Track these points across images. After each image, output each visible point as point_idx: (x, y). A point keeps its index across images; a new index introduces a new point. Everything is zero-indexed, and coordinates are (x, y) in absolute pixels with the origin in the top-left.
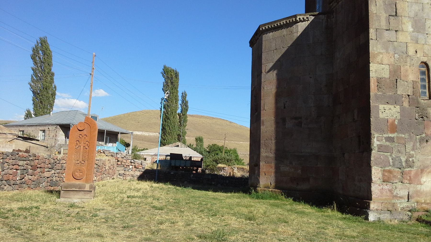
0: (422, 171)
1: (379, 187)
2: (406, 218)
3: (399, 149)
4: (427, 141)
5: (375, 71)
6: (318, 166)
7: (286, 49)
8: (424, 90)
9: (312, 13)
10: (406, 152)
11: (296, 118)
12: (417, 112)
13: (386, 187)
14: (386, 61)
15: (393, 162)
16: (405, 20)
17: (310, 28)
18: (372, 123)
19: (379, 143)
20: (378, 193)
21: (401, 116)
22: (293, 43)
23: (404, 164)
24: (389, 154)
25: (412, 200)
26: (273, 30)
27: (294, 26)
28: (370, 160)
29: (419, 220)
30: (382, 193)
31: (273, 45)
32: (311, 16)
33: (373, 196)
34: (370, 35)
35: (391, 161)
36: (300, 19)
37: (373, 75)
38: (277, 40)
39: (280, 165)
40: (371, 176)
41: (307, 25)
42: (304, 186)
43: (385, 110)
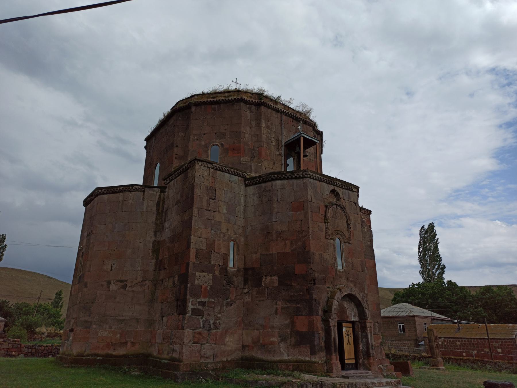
0: (226, 331)
1: (190, 349)
3: (209, 312)
5: (195, 243)
6: (138, 330)
10: (214, 315)
11: (121, 281)
12: (225, 280)
13: (196, 347)
14: (204, 236)
15: (203, 325)
20: (188, 355)
23: (212, 326)
35: (202, 323)
43: (201, 277)
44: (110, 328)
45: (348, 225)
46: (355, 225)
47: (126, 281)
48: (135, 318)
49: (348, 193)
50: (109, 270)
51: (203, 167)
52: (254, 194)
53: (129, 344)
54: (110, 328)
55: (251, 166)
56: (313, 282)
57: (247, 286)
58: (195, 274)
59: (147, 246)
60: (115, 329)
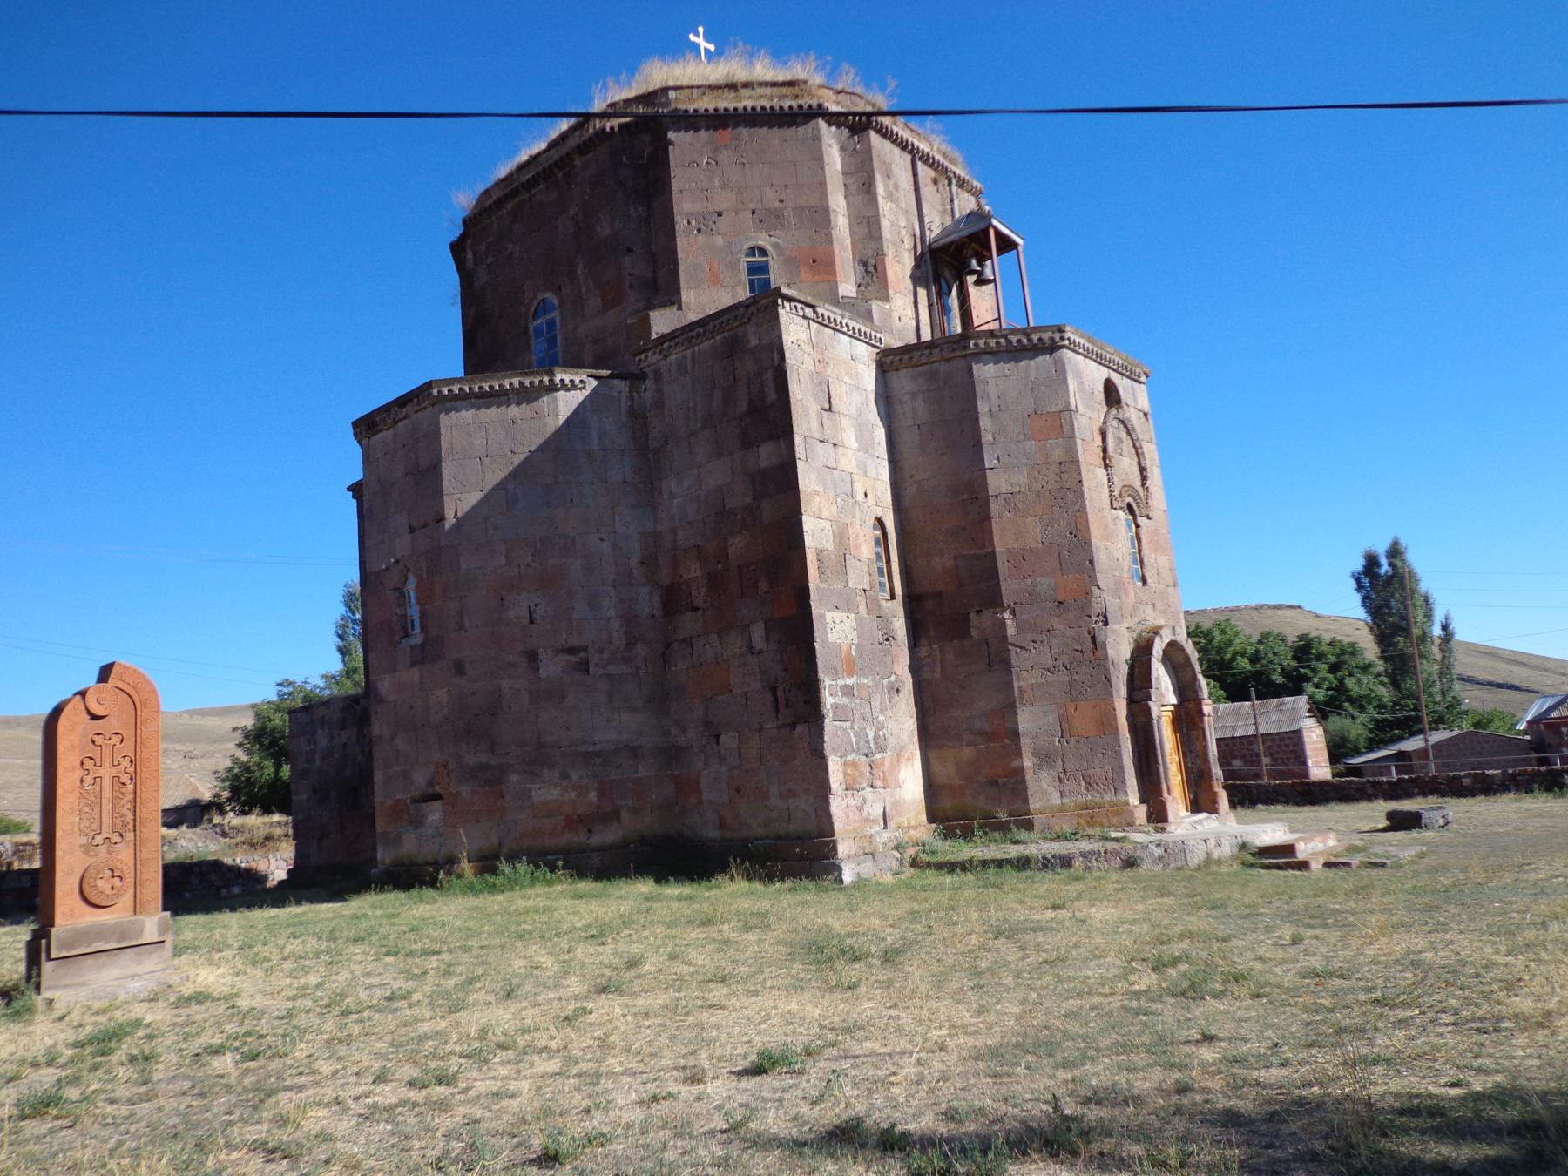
2: (895, 865)
4: (898, 691)
7: (522, 457)
8: (882, 580)
9: (594, 371)
11: (571, 651)
14: (825, 514)
16: (845, 422)
17: (588, 408)
18: (818, 655)
19: (833, 701)
21: (858, 637)
22: (545, 443)
24: (848, 724)
25: (891, 824)
26: (473, 400)
27: (545, 399)
28: (823, 741)
29: (914, 863)
30: (847, 816)
31: (479, 442)
32: (591, 379)
33: (837, 826)
34: (797, 449)
35: (853, 740)
36: (562, 380)
37: (809, 542)
38: (491, 429)
39: (528, 786)
40: (828, 780)
41: (581, 399)
42: (607, 835)
44: (565, 776)
45: (1142, 470)
46: (1152, 470)
47: (584, 649)
48: (626, 746)
49: (1132, 387)
50: (527, 621)
51: (795, 317)
52: (913, 395)
53: (625, 816)
54: (565, 776)
55: (870, 312)
56: (1101, 618)
57: (924, 641)
58: (823, 616)
59: (621, 548)
60: (581, 777)
